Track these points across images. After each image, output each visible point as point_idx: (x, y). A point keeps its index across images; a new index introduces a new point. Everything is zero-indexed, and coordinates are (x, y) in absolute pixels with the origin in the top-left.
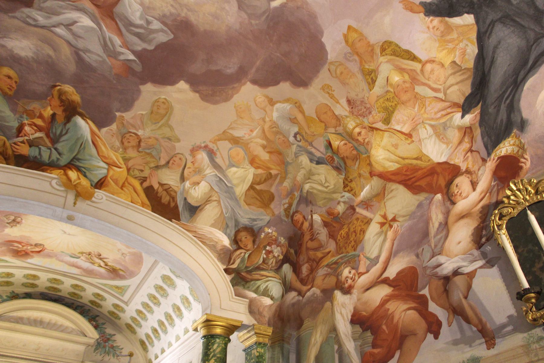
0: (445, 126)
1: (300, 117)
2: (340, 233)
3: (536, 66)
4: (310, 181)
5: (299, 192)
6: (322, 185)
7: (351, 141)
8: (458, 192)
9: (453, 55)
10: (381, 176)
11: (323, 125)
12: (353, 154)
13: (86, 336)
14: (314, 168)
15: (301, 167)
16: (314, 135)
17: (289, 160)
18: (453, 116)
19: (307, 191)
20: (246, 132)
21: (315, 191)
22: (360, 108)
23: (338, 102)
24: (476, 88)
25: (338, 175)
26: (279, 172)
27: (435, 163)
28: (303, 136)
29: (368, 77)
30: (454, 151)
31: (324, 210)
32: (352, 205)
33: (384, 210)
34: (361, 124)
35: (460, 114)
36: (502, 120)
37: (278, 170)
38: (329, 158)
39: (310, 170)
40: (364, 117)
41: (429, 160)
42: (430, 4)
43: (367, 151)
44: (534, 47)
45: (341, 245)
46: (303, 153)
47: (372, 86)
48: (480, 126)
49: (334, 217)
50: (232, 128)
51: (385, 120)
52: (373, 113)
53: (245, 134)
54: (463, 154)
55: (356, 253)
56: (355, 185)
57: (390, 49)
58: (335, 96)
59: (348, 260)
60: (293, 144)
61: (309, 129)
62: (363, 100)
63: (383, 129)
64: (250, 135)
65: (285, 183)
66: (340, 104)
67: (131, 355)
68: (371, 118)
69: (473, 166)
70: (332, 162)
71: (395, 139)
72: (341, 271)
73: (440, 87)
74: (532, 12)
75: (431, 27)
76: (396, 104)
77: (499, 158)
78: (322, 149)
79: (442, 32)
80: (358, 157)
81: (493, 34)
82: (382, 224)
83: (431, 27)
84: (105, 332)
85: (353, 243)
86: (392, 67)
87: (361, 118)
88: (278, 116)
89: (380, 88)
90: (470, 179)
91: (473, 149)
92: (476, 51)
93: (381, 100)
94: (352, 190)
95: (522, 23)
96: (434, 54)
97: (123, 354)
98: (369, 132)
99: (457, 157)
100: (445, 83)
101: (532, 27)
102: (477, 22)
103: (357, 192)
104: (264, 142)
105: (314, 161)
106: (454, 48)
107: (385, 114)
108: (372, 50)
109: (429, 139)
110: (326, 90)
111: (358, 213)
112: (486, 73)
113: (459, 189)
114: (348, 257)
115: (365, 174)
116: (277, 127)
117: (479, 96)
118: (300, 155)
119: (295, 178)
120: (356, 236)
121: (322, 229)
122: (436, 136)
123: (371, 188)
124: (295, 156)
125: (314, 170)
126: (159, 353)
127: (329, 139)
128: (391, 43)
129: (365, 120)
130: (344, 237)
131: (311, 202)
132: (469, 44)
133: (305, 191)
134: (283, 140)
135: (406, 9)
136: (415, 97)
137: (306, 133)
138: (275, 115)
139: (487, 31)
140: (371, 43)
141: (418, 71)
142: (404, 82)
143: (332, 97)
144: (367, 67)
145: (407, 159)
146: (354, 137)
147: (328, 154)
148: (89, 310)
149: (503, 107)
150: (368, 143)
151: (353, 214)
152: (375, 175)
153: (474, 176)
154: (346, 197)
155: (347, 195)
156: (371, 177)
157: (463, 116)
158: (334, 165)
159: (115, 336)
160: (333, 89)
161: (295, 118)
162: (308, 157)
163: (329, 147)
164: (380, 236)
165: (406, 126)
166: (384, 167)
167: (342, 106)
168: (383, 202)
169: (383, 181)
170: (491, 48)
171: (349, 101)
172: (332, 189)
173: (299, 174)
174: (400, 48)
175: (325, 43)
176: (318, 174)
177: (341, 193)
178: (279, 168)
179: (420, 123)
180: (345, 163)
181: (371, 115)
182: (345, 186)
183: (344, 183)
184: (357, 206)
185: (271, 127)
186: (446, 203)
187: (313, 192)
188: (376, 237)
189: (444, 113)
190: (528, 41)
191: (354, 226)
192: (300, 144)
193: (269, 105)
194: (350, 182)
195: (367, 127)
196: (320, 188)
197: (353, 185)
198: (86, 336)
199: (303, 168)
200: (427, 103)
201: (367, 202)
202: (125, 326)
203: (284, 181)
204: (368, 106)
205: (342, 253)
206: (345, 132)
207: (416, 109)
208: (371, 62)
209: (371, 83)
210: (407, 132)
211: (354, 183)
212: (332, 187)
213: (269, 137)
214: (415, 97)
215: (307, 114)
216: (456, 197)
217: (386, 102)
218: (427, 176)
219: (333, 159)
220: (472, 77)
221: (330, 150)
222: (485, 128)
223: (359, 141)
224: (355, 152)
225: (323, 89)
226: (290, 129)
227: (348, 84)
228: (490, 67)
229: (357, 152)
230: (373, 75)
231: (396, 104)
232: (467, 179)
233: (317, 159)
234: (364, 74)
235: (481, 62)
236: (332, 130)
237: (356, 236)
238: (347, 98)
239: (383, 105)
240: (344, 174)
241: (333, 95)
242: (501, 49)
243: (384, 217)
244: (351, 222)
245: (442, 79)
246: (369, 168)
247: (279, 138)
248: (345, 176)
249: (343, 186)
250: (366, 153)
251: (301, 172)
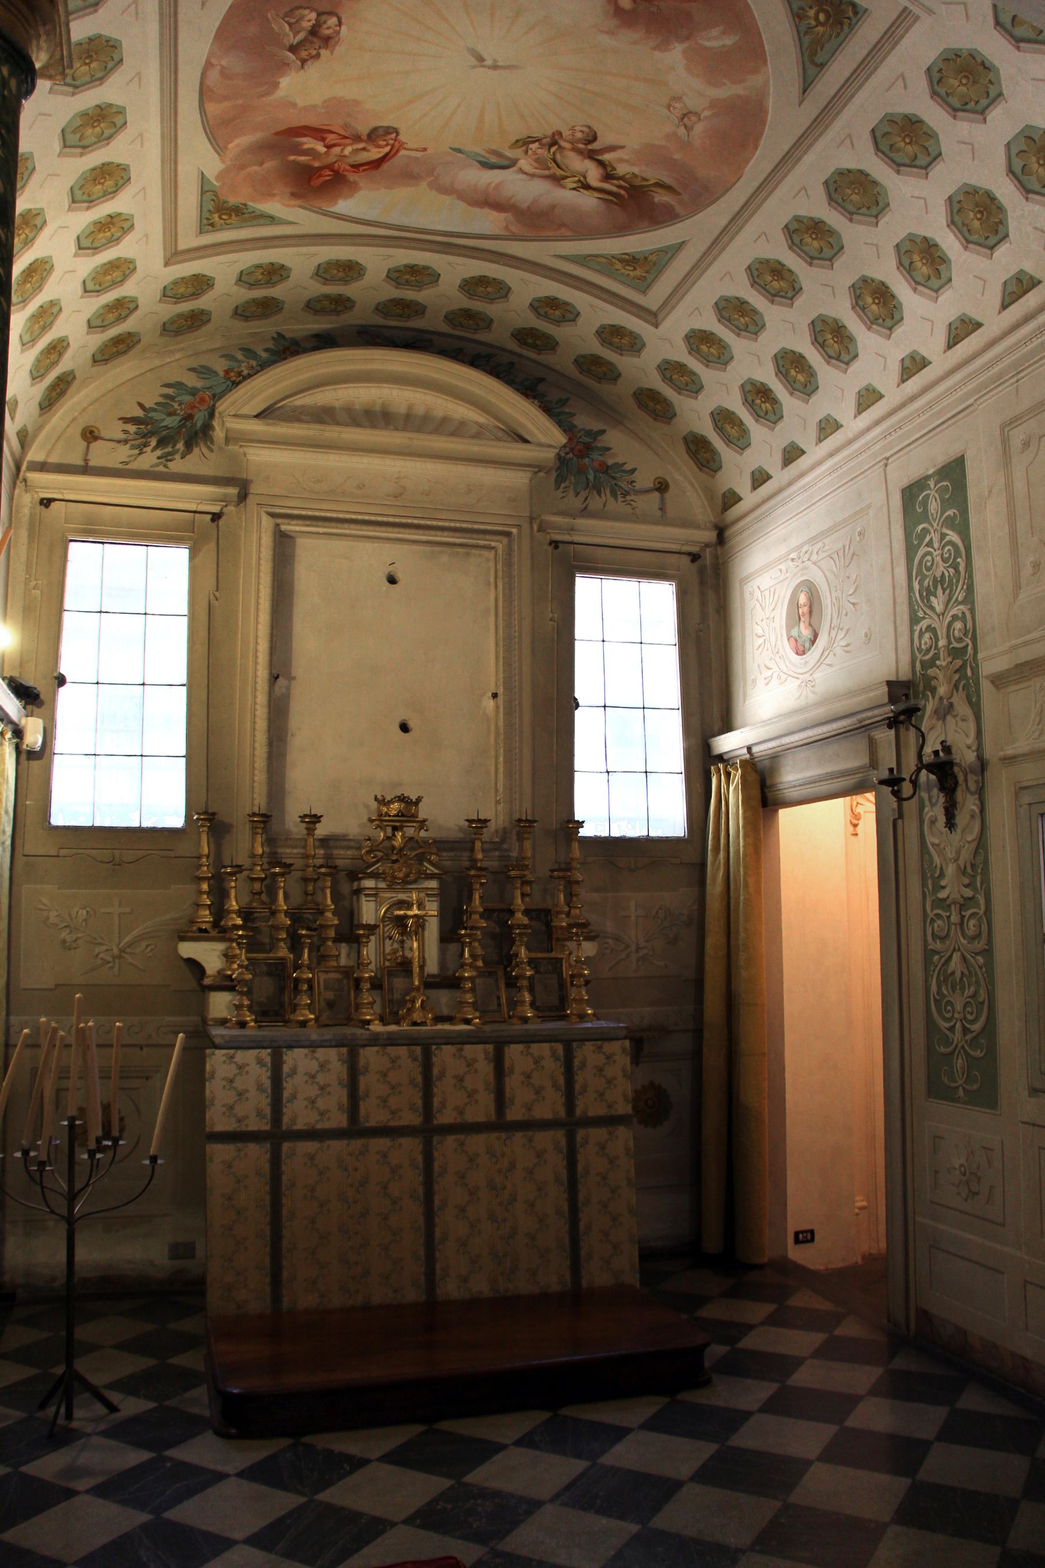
13: (526, 441)
67: (662, 487)
84: (575, 426)
97: (638, 486)
126: (772, 463)
148: (512, 364)
159: (604, 437)
198: (526, 441)
202: (631, 402)
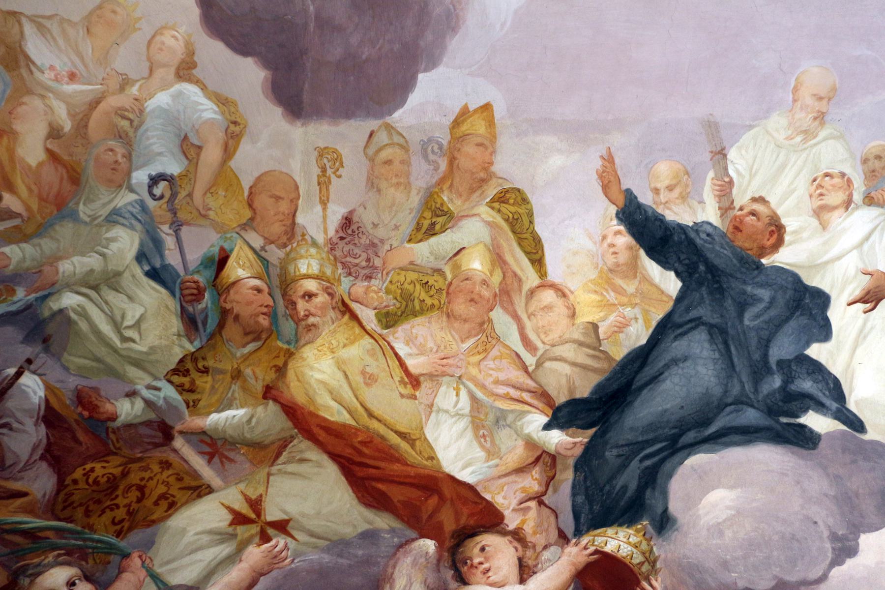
0: (500, 419)
1: (212, 155)
2: (88, 467)
3: (720, 441)
4: (92, 293)
5: (33, 296)
6: (117, 327)
7: (278, 294)
8: (481, 563)
9: (602, 314)
10: (291, 411)
11: (248, 214)
12: (257, 322)
14: (133, 276)
15: (99, 248)
16: (205, 216)
17: (83, 211)
18: (529, 412)
19: (61, 311)
20: (58, 68)
21: (83, 326)
22: (356, 251)
23: (324, 203)
24: (601, 398)
25: (179, 335)
26: (25, 214)
27: (443, 473)
28: (174, 195)
29: (428, 214)
30: (499, 477)
31: (73, 382)
32: (169, 422)
33: (261, 490)
34: (328, 281)
35: (544, 419)
36: (625, 488)
37: (28, 208)
38: (193, 285)
39: (118, 274)
40: (350, 274)
41: (432, 458)
42: (639, 206)
43: (296, 341)
44: (728, 409)
45: (76, 498)
46: (139, 226)
47: (420, 236)
48: (577, 468)
49: (91, 417)
50: (41, 29)
51: (387, 314)
52: (373, 281)
53: (52, 68)
54: (520, 496)
55: (122, 544)
56: (208, 386)
57: (513, 209)
58: (332, 189)
59: (80, 548)
60: (131, 190)
61: (205, 194)
62: (379, 244)
63: (368, 328)
64: (56, 80)
65: (14, 247)
66: (324, 209)
68: (360, 288)
69: (535, 533)
70: (190, 298)
71: (377, 365)
72: (39, 565)
73: (539, 345)
74: (757, 356)
75: (609, 240)
76: (433, 305)
77: (596, 552)
78: (194, 256)
79: (618, 265)
80: (264, 336)
81: (686, 338)
82: (239, 519)
83: (609, 240)
85: (121, 513)
86: (488, 240)
87: (340, 271)
88: (166, 107)
89: (431, 253)
90: (520, 553)
91: (545, 499)
92: (643, 341)
93: (412, 276)
94: (191, 391)
95: (736, 360)
96: (572, 284)
98: (334, 308)
99: (503, 494)
100: (553, 346)
101: (744, 378)
102: (679, 299)
103: (202, 404)
104: (67, 126)
105: (150, 264)
106: (614, 305)
107: (398, 305)
108: (483, 181)
109: (453, 417)
110: (325, 161)
111: (175, 451)
112: (634, 387)
113: (487, 559)
114: (85, 540)
115: (253, 381)
116: (135, 123)
117: (598, 414)
118: (123, 225)
119: (56, 258)
120: (139, 500)
121: (29, 424)
122: (473, 422)
123: (249, 421)
124: (110, 214)
125: (126, 281)
127: (232, 250)
128: (525, 200)
129: (346, 282)
130: (96, 482)
131: (45, 341)
132: (640, 321)
133: (54, 305)
134: (116, 162)
135: (600, 177)
136: (482, 324)
137: (190, 195)
138: (162, 99)
139: (680, 326)
140: (495, 168)
141: (526, 288)
142: (484, 282)
143: (324, 183)
144: (445, 199)
145: (380, 421)
146: (291, 293)
147: (196, 277)
149: (635, 467)
150: (309, 328)
151: (157, 446)
152: (275, 400)
153: (529, 553)
154: (162, 394)
155: (169, 391)
156: (265, 397)
157: (547, 427)
158: (190, 309)
160: (341, 171)
161: (200, 148)
162: (142, 245)
163: (215, 267)
164: (222, 542)
165: (422, 359)
166: (312, 401)
167: (325, 218)
168: (267, 470)
169: (289, 424)
170: (667, 357)
171: (347, 222)
172: (141, 352)
173: (76, 259)
174: (531, 222)
175: (419, 84)
176: (130, 298)
177: (156, 378)
178: (35, 206)
179: (452, 376)
180: (221, 326)
181: (366, 284)
182: (180, 369)
183: (181, 361)
184: (181, 432)
185: (121, 113)
186: (442, 569)
187: (76, 323)
188: (206, 538)
189: (514, 393)
190: (726, 392)
191: (147, 475)
192: (151, 204)
193: (173, 70)
194: (199, 371)
195: (337, 298)
196: (106, 328)
197: (204, 382)
199: (103, 255)
200: (495, 352)
201: (219, 443)
203: (17, 242)
204: (378, 262)
205: (69, 520)
206: (281, 269)
207: (465, 346)
208: (461, 196)
209: (424, 229)
210: (413, 370)
211: (209, 379)
212: (141, 348)
213: (92, 124)
214: (482, 324)
215: (232, 164)
216: (474, 571)
217: (418, 287)
218: (412, 485)
219: (199, 295)
220: (606, 375)
221: (210, 273)
222: (585, 478)
223: (295, 309)
224: (264, 321)
225: (322, 153)
226: (160, 154)
227: (379, 191)
228: (646, 384)
229: (271, 324)
230: (441, 220)
231: (433, 305)
232: (513, 550)
233: (158, 264)
234: (426, 203)
235: (637, 365)
236: (257, 242)
237: (139, 500)
238: (351, 212)
239: (406, 286)
240: (197, 344)
241: (330, 182)
242: (680, 371)
243: (256, 505)
244: (140, 460)
245: (554, 336)
246: (271, 375)
247: (112, 150)
248: (197, 350)
249: (173, 366)
250: (288, 343)
251: (85, 260)
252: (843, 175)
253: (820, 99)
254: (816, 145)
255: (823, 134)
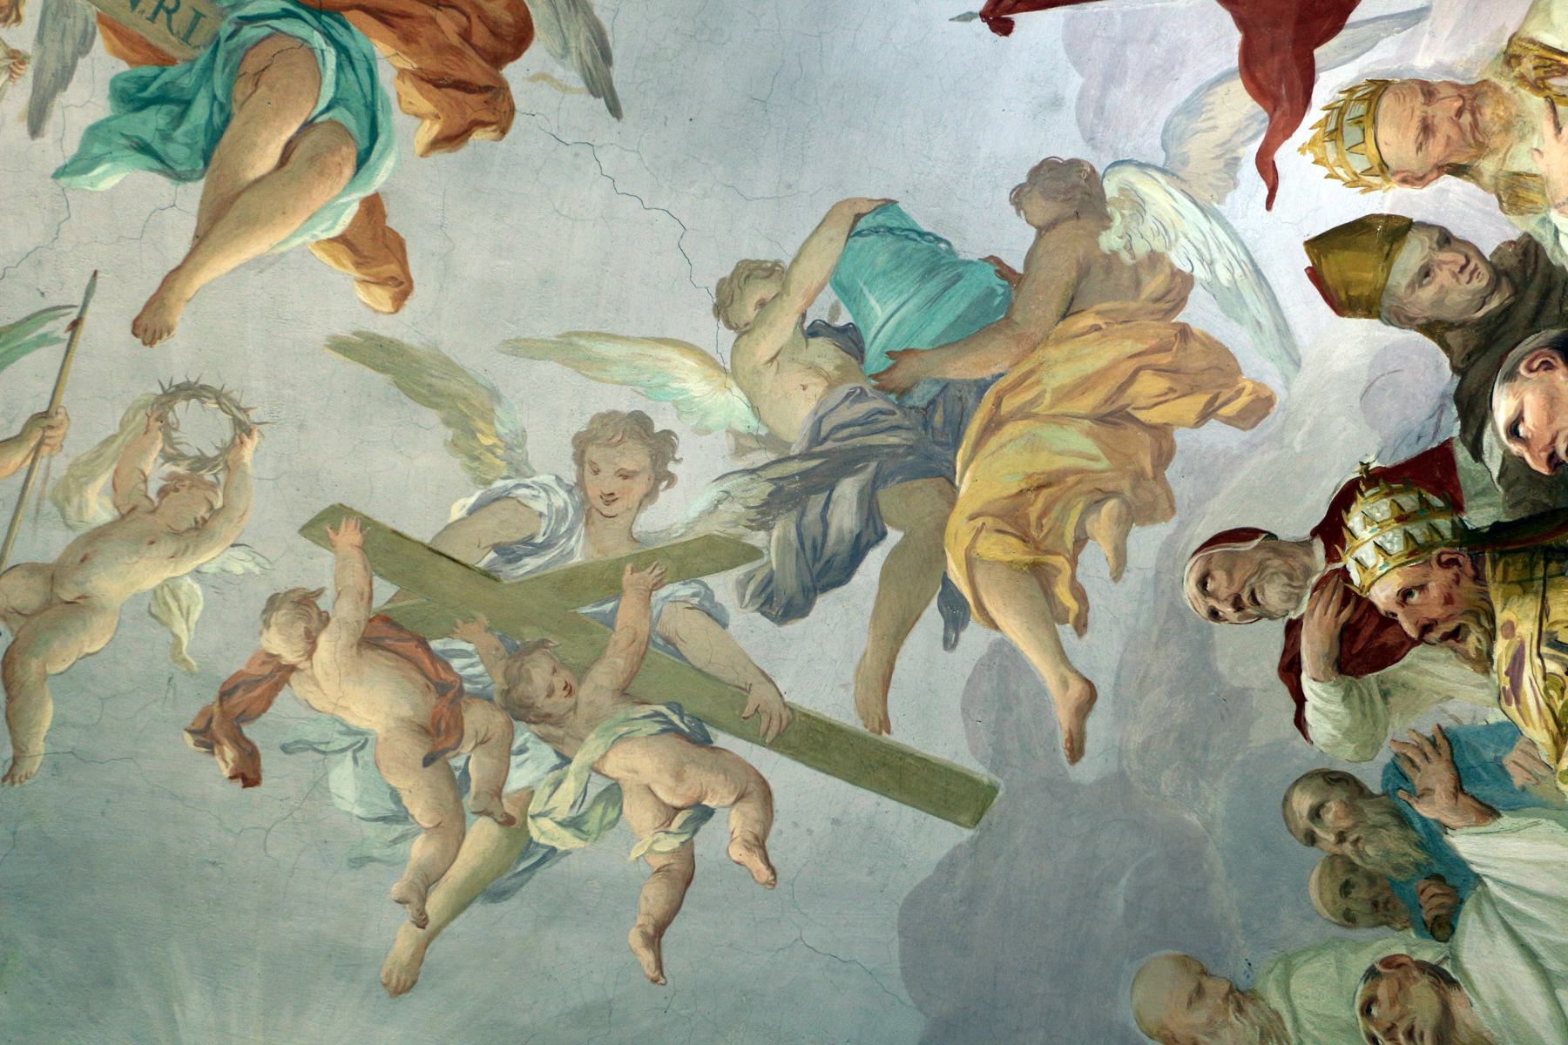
252: (1372, 974)
253: (1200, 991)
254: (1295, 1020)
255: (1275, 1000)
